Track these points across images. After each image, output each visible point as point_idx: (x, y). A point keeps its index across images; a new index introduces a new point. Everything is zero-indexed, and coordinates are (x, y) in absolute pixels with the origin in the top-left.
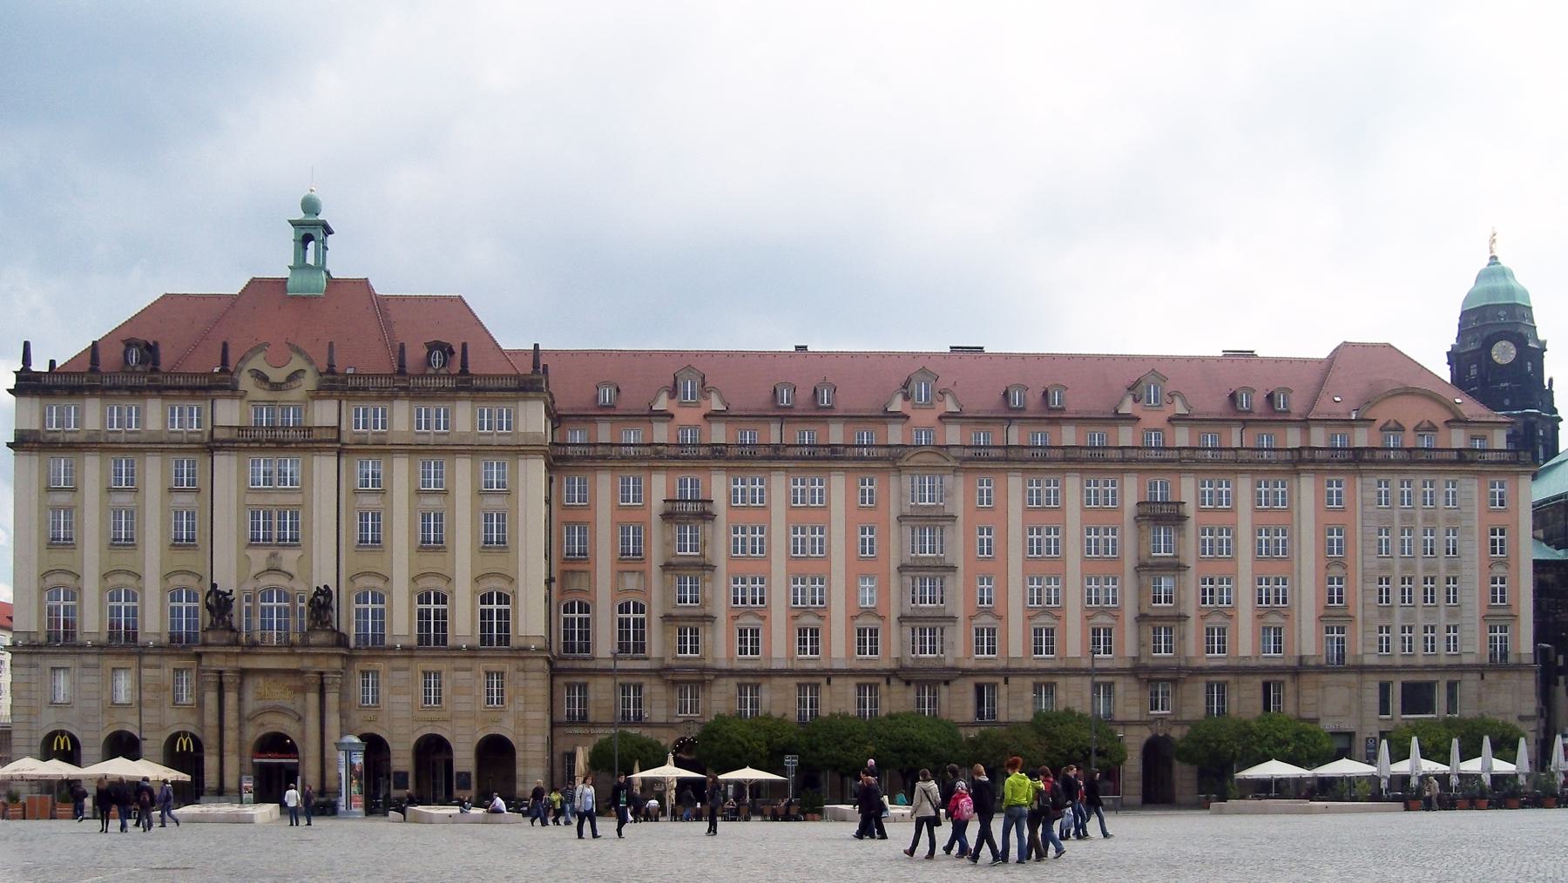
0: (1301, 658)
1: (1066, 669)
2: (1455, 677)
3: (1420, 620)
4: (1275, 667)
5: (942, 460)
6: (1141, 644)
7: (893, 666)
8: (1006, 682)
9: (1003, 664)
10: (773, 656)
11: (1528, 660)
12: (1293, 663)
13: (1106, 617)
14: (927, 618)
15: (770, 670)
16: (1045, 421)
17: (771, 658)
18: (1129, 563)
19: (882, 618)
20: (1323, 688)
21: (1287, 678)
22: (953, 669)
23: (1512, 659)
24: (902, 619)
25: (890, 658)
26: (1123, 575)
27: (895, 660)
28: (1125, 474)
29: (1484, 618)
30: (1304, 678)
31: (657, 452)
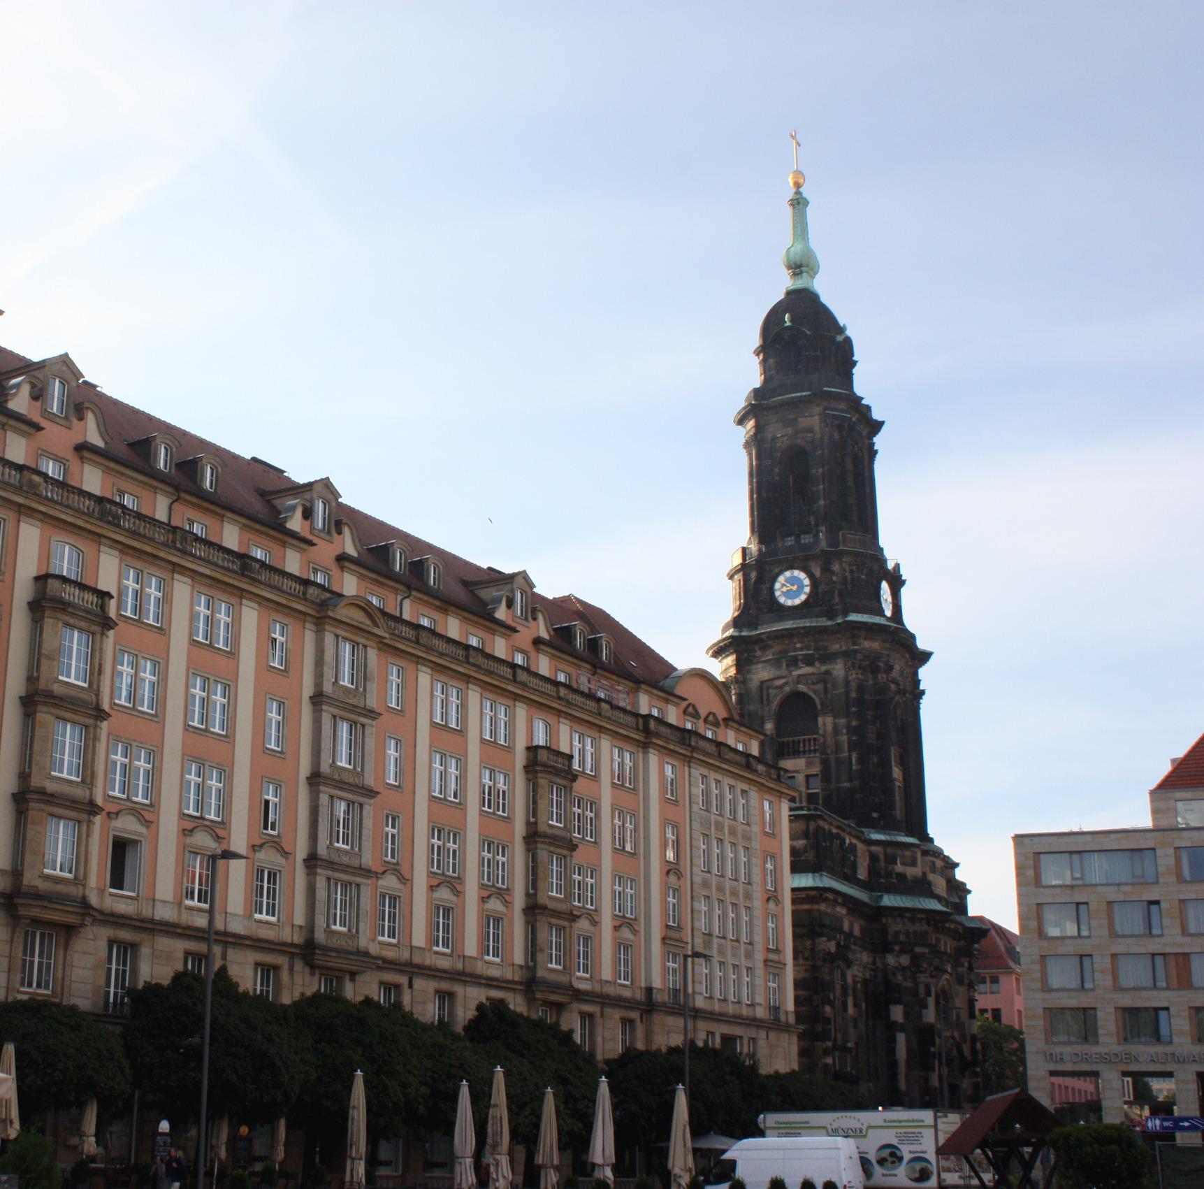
0: (649, 990)
1: (462, 973)
2: (752, 1032)
3: (731, 960)
4: (625, 1000)
5: (368, 622)
6: (533, 947)
7: (298, 939)
8: (411, 986)
9: (405, 955)
10: (158, 896)
11: (792, 1020)
12: (640, 996)
13: (498, 902)
14: (345, 868)
15: (152, 921)
16: (438, 603)
17: (154, 900)
18: (519, 829)
19: (285, 854)
20: (668, 1033)
21: (635, 1015)
22: (366, 954)
23: (783, 1018)
24: (312, 861)
25: (293, 925)
26: (513, 843)
27: (298, 929)
28: (518, 704)
29: (766, 961)
30: (657, 1018)
31: (32, 485)
